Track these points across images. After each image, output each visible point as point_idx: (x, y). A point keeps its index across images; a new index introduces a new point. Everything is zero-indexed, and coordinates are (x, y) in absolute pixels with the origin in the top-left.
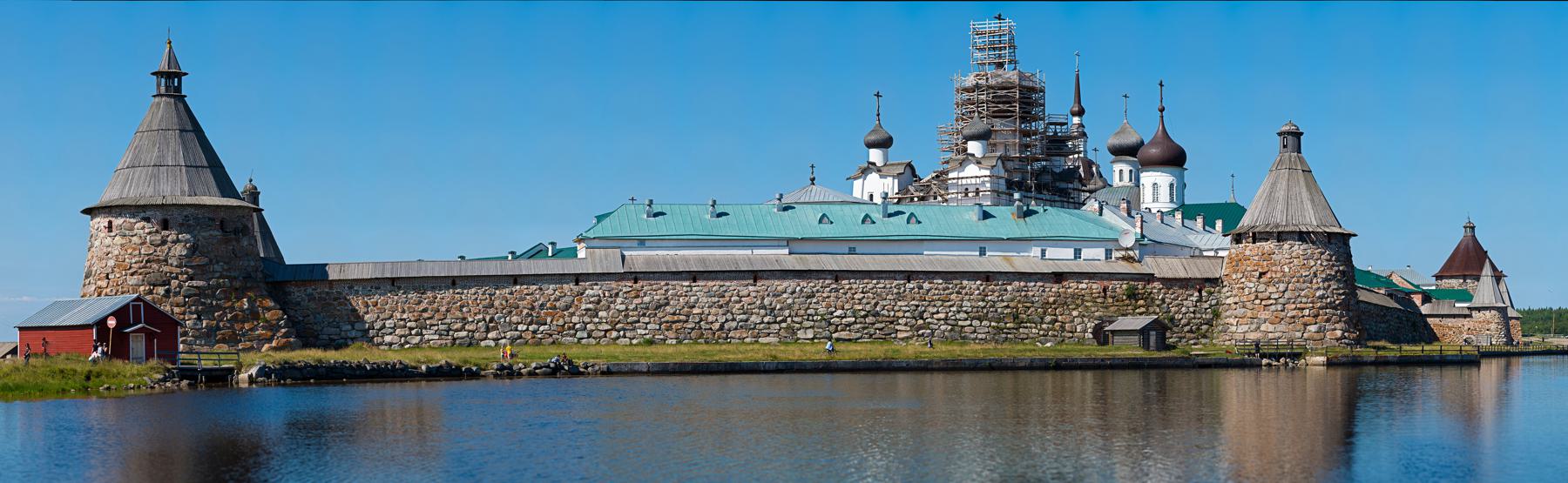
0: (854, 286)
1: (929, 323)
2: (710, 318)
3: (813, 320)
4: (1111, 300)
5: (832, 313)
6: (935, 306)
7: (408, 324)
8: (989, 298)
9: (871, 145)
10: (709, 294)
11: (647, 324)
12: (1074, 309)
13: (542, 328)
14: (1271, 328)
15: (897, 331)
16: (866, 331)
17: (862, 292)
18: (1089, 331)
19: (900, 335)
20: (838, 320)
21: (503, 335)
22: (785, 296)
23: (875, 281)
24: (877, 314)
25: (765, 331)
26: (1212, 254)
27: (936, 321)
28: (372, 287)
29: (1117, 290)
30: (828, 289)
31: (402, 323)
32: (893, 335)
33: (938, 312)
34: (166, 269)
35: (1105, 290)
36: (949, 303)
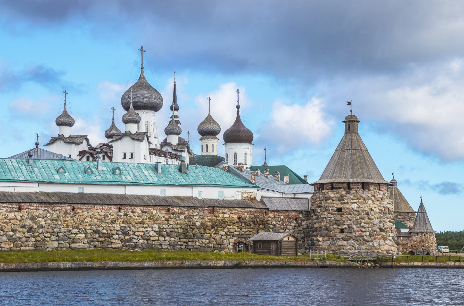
0: (86, 214)
1: (133, 238)
3: (58, 236)
4: (243, 225)
5: (69, 231)
6: (135, 227)
8: (170, 222)
9: (59, 124)
12: (221, 230)
14: (345, 243)
15: (112, 243)
16: (92, 243)
17: (90, 218)
18: (231, 244)
19: (114, 246)
20: (74, 235)
22: (40, 219)
23: (99, 211)
24: (97, 232)
26: (293, 196)
27: (136, 237)
29: (247, 218)
30: (68, 215)
32: (110, 246)
35: (239, 218)
36: (145, 225)
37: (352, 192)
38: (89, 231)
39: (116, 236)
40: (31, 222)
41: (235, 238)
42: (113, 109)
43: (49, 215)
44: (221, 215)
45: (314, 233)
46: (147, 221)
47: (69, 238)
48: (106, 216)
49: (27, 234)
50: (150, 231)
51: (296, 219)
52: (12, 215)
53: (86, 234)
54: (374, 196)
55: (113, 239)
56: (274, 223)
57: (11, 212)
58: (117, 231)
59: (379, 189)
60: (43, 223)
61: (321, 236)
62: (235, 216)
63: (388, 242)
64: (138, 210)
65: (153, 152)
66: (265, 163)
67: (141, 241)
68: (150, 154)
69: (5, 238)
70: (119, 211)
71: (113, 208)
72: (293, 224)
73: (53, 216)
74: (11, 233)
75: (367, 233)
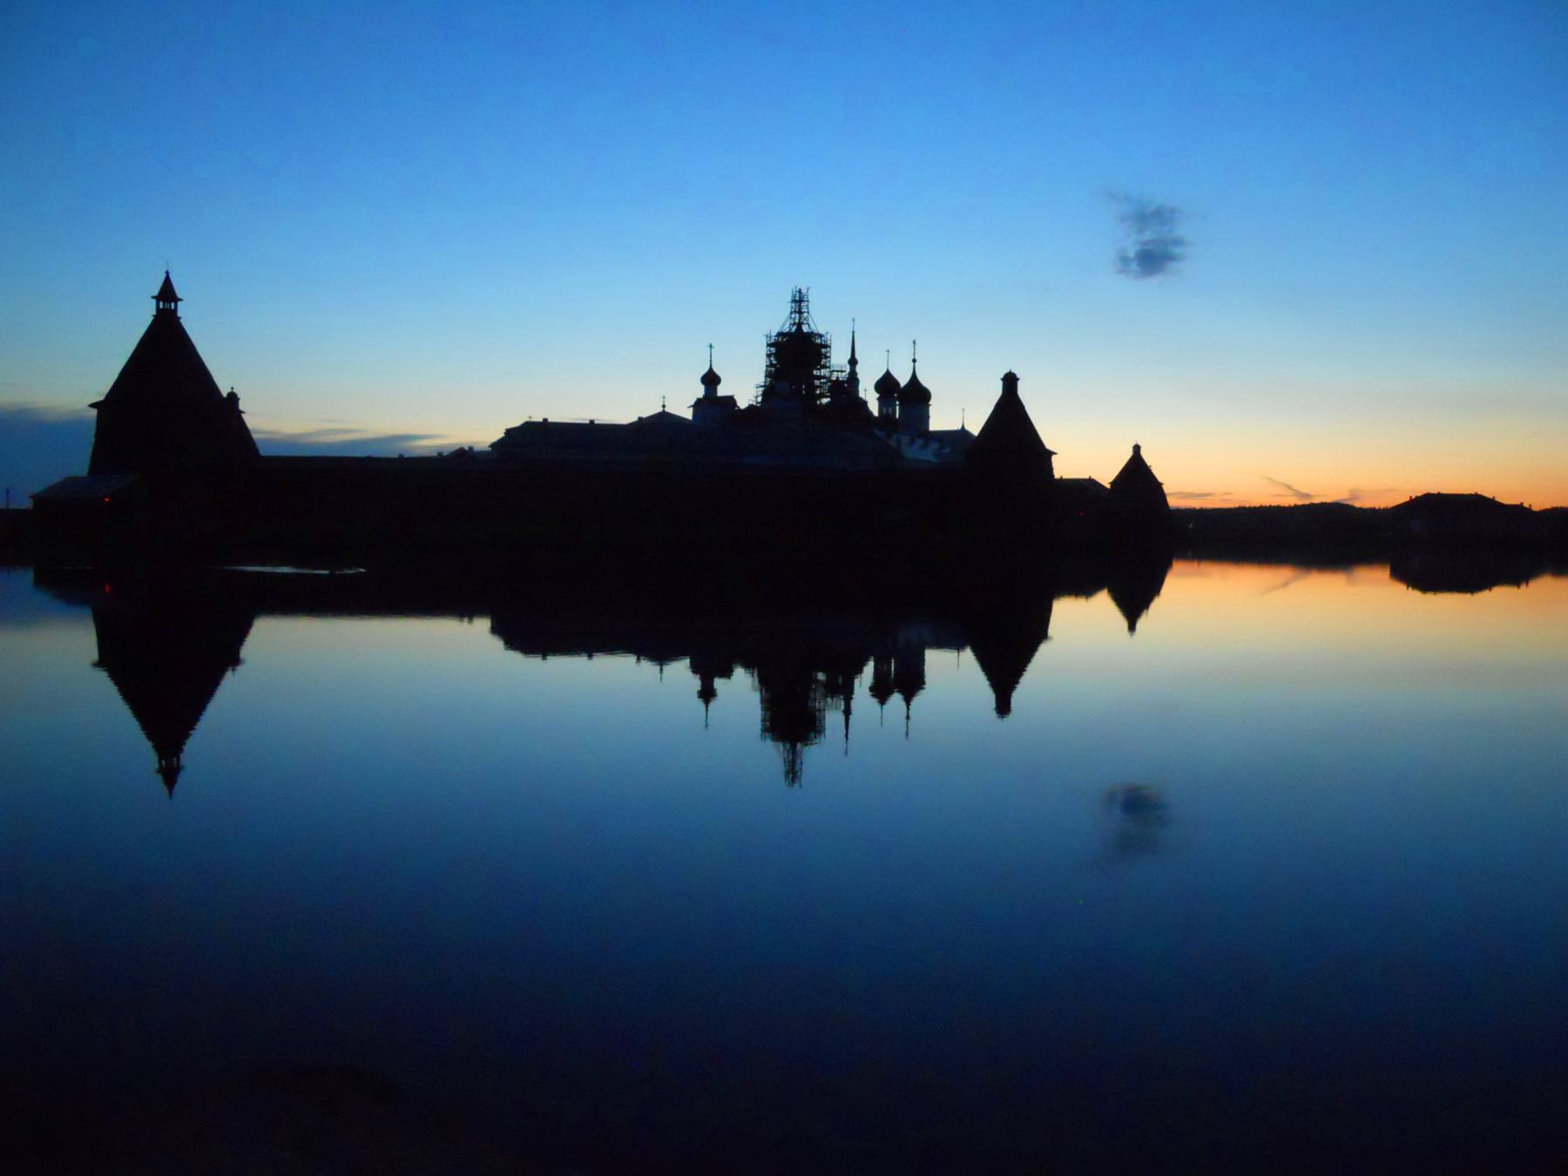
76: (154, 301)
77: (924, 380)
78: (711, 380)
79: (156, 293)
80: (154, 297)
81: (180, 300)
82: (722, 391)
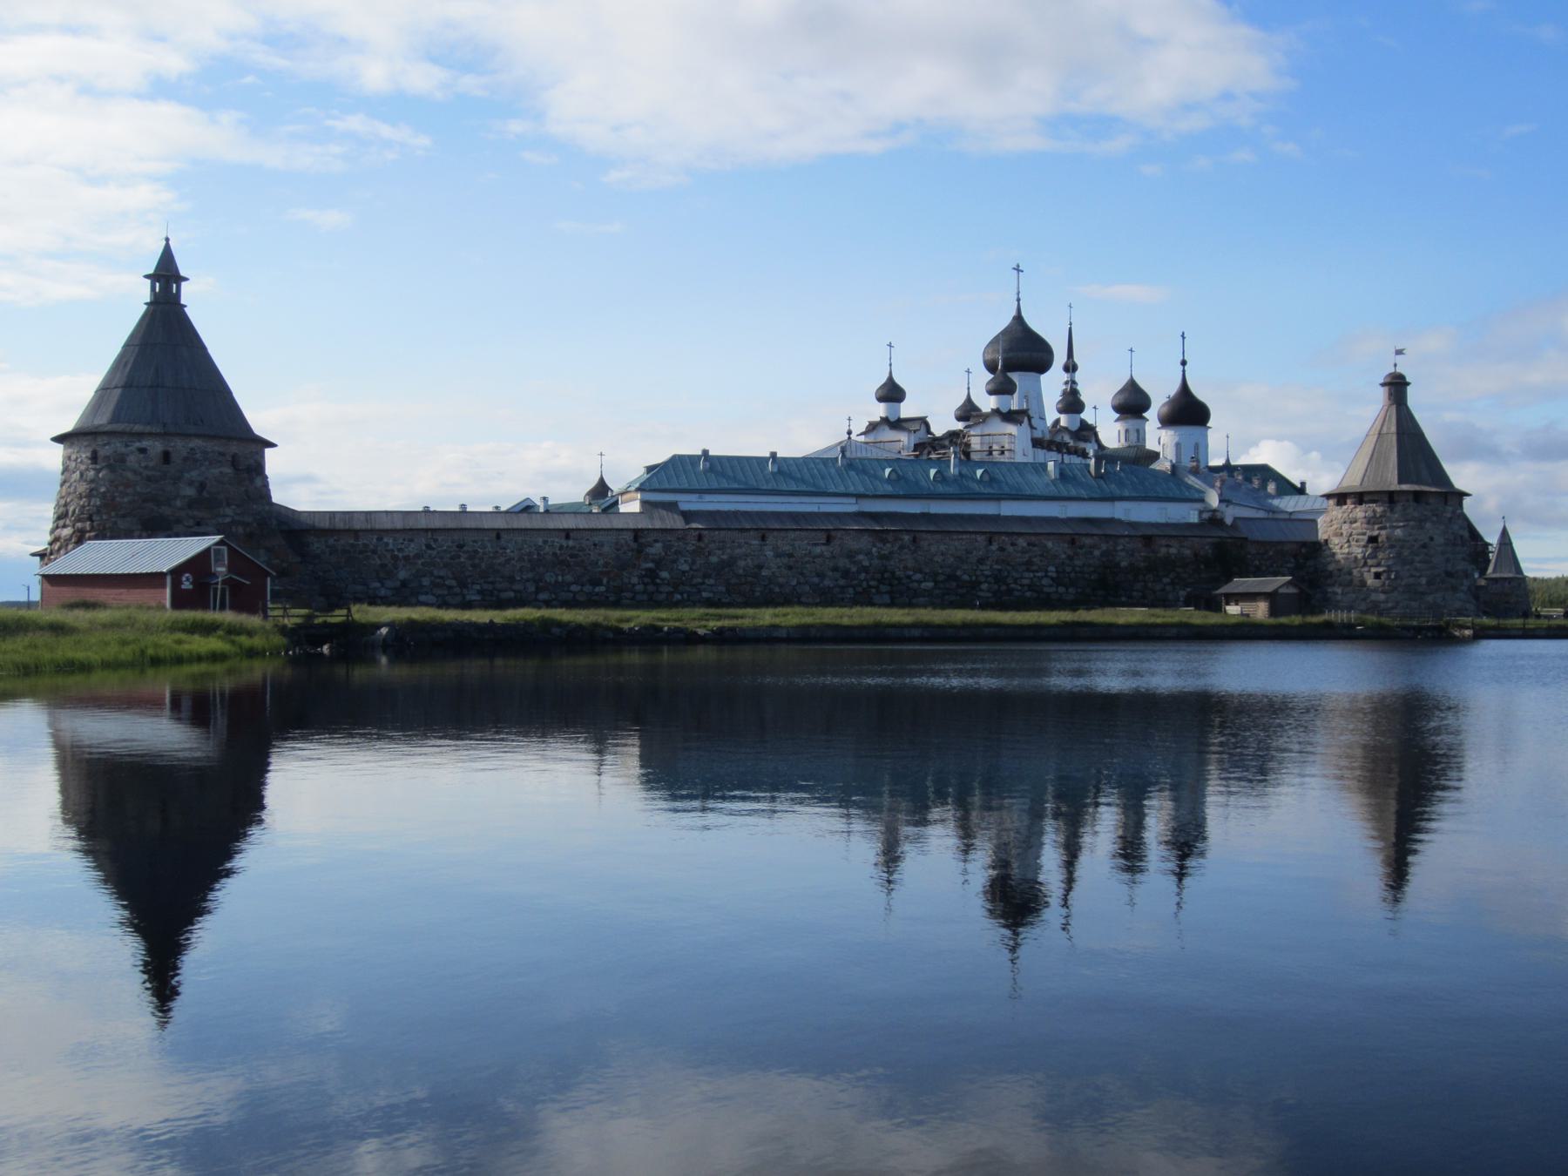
1: (1013, 590)
2: (781, 580)
5: (909, 577)
7: (447, 582)
10: (778, 555)
11: (712, 586)
13: (597, 589)
16: (947, 597)
20: (916, 585)
21: (553, 596)
22: (861, 557)
23: (956, 543)
25: (840, 596)
27: (1020, 588)
28: (404, 540)
30: (906, 550)
31: (438, 580)
33: (1022, 578)
34: (166, 511)
35: (1196, 555)
37: (1399, 508)
38: (941, 578)
39: (984, 586)
40: (847, 561)
41: (1189, 590)
42: (968, 372)
43: (874, 550)
44: (1164, 550)
45: (1329, 581)
46: (1035, 560)
47: (908, 588)
48: (968, 552)
49: (842, 582)
50: (1042, 577)
51: (1295, 556)
52: (818, 550)
53: (936, 582)
54: (1437, 515)
55: (981, 590)
56: (1257, 563)
57: (816, 545)
58: (987, 576)
59: (1446, 503)
60: (866, 563)
61: (1340, 585)
62: (1188, 552)
63: (1461, 595)
64: (1022, 542)
65: (1037, 443)
66: (1228, 460)
67: (1028, 594)
68: (1034, 446)
69: (807, 588)
70: (990, 542)
71: (980, 538)
72: (1289, 565)
73: (883, 552)
74: (816, 580)
75: (1424, 581)
76: (148, 282)
77: (1200, 392)
78: (892, 393)
79: (151, 271)
80: (147, 277)
81: (186, 279)
82: (907, 410)
